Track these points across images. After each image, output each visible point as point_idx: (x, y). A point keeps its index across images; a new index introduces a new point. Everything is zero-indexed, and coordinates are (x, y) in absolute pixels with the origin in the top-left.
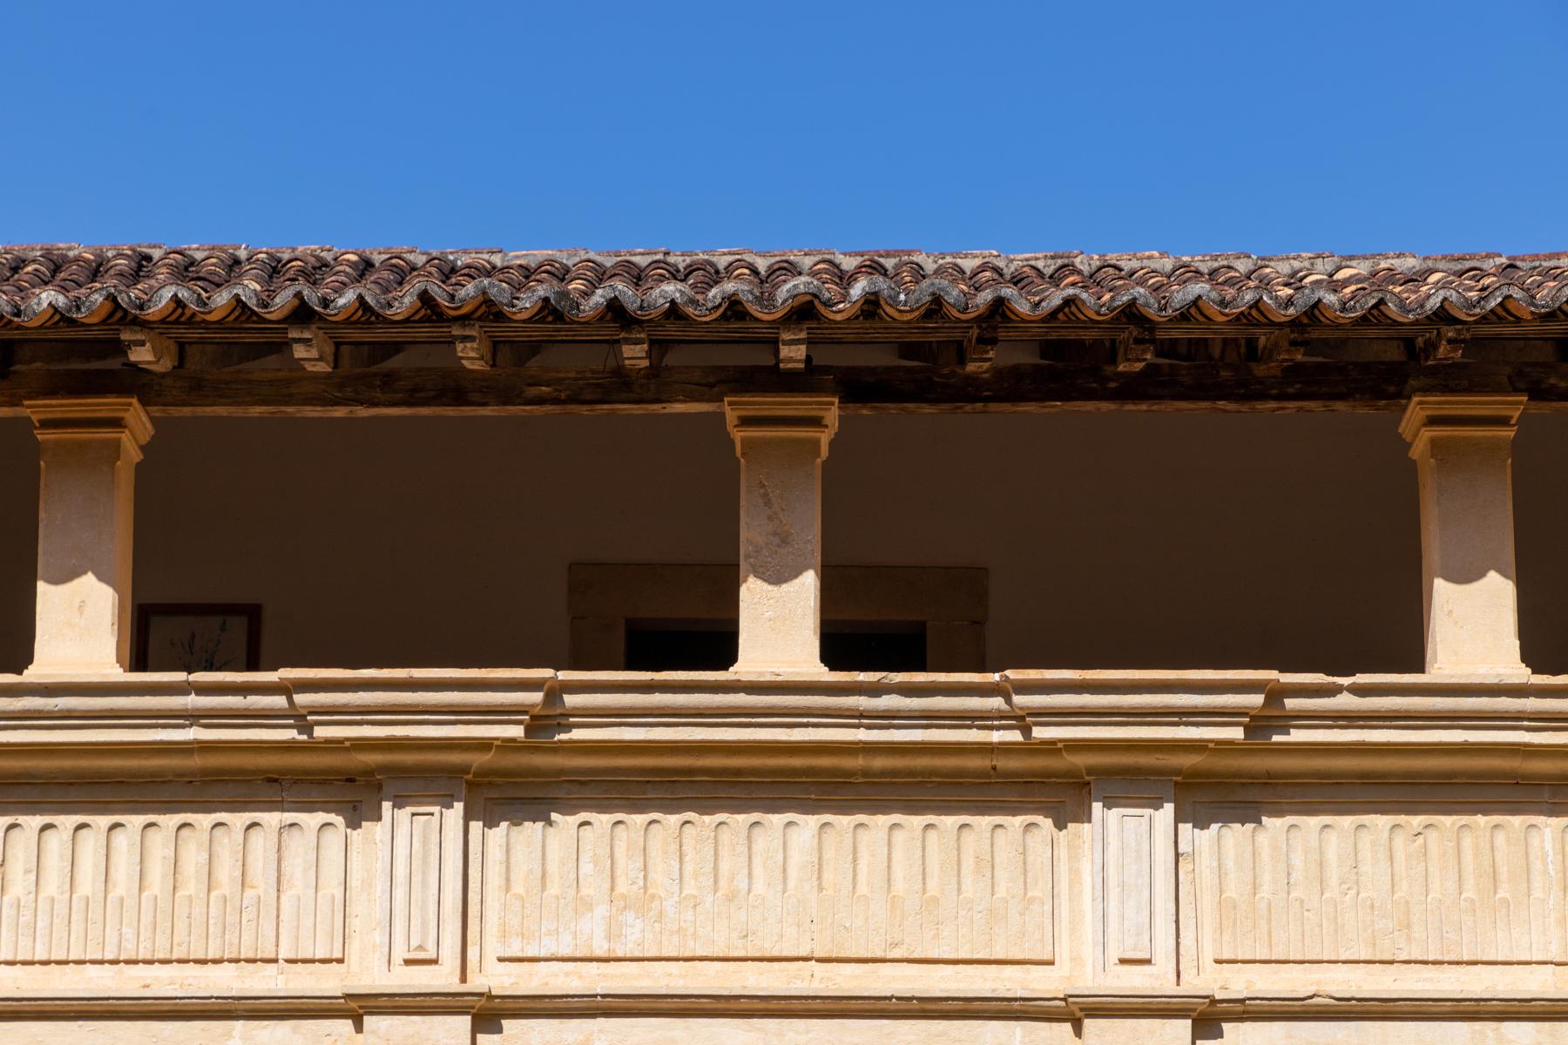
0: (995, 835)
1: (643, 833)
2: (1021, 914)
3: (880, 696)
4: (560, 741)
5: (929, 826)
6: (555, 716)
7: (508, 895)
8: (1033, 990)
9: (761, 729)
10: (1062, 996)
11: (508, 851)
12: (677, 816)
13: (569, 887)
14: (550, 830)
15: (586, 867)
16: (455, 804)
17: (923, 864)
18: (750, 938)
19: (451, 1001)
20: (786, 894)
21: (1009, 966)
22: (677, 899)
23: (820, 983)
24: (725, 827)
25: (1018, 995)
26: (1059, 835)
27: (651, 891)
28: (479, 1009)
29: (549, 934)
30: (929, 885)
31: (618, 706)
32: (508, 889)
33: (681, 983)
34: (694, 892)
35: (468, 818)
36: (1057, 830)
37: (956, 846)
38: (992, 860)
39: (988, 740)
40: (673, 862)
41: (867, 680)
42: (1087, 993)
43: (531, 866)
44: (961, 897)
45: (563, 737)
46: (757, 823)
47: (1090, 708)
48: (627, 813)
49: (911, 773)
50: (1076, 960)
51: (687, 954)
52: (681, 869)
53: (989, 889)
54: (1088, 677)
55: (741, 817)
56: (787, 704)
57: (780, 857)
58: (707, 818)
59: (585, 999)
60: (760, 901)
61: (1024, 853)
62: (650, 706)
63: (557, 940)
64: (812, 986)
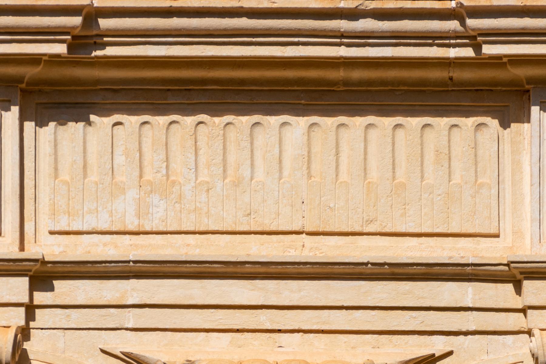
0: (452, 132)
1: (165, 132)
2: (473, 197)
3: (358, 20)
4: (96, 57)
5: (398, 126)
6: (92, 37)
7: (56, 181)
8: (482, 257)
9: (260, 47)
10: (506, 262)
11: (56, 146)
12: (193, 118)
13: (105, 175)
14: (90, 129)
15: (120, 159)
16: (12, 108)
17: (393, 156)
18: (253, 216)
19: (11, 265)
20: (281, 181)
21: (463, 238)
22: (193, 184)
23: (310, 252)
24: (231, 127)
25: (470, 262)
26: (503, 133)
27: (172, 178)
28: (36, 272)
29: (90, 212)
30: (398, 174)
31: (143, 28)
32: (56, 177)
33: (197, 251)
34: (207, 179)
35: (22, 119)
36: (502, 129)
37: (420, 141)
38: (449, 153)
39: (446, 55)
40: (190, 155)
41: (346, 6)
42: (526, 260)
43: (75, 158)
44: (424, 183)
45: (99, 53)
46: (257, 123)
47: (530, 29)
48: (152, 116)
49: (383, 82)
50: (518, 233)
51: (202, 229)
52: (196, 160)
53: (447, 176)
54: (528, 4)
55: (244, 119)
56: (281, 26)
57: (277, 151)
58: (217, 120)
59: (120, 264)
60: (260, 186)
61: (475, 148)
62: (169, 28)
63: (97, 217)
64: (303, 254)
